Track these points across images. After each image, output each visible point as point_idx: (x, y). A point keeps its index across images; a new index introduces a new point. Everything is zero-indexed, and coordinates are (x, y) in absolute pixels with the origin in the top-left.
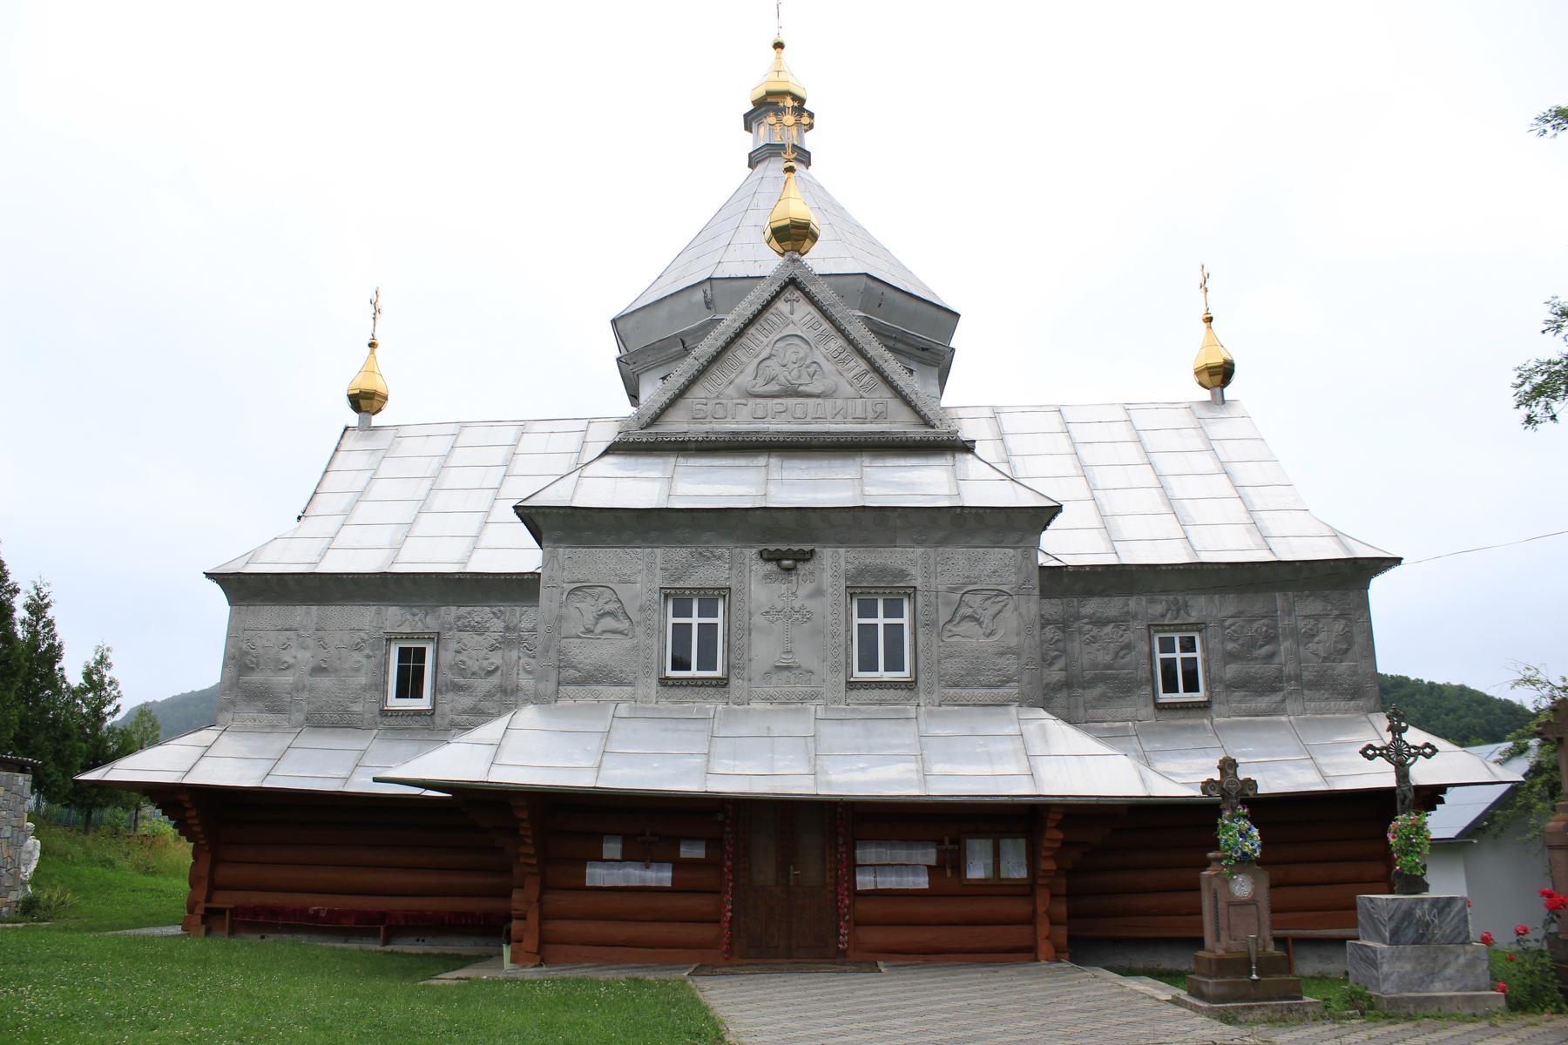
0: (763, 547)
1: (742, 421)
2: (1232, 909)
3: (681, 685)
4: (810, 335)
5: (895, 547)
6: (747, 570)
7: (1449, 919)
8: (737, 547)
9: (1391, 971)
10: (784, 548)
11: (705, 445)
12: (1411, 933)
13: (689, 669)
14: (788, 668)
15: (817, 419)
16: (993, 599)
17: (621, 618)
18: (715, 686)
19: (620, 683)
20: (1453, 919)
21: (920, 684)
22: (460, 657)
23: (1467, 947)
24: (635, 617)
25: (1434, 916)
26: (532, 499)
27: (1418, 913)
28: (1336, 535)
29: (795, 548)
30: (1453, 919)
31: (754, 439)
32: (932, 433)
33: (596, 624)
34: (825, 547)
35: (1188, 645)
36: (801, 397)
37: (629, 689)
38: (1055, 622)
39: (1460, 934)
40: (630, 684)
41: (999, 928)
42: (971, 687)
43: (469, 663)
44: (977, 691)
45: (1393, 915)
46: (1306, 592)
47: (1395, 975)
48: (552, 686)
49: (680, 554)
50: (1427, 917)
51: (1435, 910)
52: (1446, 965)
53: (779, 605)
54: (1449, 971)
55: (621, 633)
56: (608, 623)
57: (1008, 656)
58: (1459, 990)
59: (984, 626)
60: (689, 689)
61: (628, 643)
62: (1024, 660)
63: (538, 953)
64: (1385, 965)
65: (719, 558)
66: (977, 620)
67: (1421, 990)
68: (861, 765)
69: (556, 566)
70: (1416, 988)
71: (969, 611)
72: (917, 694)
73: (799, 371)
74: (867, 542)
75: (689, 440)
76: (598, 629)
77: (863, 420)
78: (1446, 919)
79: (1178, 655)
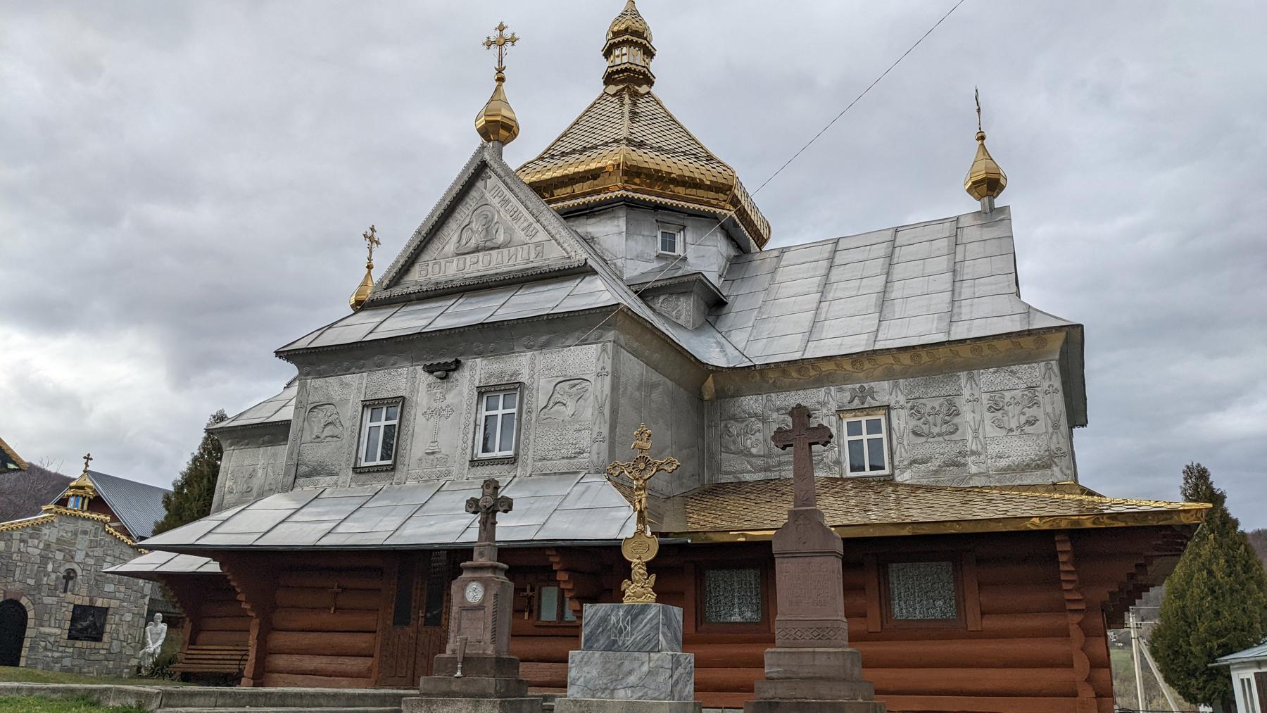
2: (464, 613)
3: (365, 472)
5: (514, 353)
6: (417, 382)
7: (641, 626)
8: (412, 366)
9: (579, 675)
12: (602, 641)
13: (375, 460)
16: (577, 387)
17: (338, 426)
18: (387, 470)
19: (331, 474)
23: (652, 654)
24: (347, 424)
25: (628, 623)
27: (613, 619)
29: (442, 361)
33: (323, 431)
34: (468, 359)
35: (874, 427)
36: (488, 250)
37: (336, 477)
38: (756, 415)
39: (649, 641)
40: (337, 474)
45: (589, 621)
46: (991, 370)
47: (582, 679)
48: (291, 478)
50: (621, 624)
51: (629, 617)
52: (630, 673)
54: (632, 679)
56: (329, 430)
57: (583, 432)
59: (569, 409)
62: (595, 435)
63: (252, 679)
64: (573, 670)
66: (565, 405)
67: (603, 696)
68: (432, 523)
70: (599, 694)
72: (517, 467)
74: (496, 353)
75: (410, 293)
76: (323, 437)
78: (638, 626)
79: (865, 437)
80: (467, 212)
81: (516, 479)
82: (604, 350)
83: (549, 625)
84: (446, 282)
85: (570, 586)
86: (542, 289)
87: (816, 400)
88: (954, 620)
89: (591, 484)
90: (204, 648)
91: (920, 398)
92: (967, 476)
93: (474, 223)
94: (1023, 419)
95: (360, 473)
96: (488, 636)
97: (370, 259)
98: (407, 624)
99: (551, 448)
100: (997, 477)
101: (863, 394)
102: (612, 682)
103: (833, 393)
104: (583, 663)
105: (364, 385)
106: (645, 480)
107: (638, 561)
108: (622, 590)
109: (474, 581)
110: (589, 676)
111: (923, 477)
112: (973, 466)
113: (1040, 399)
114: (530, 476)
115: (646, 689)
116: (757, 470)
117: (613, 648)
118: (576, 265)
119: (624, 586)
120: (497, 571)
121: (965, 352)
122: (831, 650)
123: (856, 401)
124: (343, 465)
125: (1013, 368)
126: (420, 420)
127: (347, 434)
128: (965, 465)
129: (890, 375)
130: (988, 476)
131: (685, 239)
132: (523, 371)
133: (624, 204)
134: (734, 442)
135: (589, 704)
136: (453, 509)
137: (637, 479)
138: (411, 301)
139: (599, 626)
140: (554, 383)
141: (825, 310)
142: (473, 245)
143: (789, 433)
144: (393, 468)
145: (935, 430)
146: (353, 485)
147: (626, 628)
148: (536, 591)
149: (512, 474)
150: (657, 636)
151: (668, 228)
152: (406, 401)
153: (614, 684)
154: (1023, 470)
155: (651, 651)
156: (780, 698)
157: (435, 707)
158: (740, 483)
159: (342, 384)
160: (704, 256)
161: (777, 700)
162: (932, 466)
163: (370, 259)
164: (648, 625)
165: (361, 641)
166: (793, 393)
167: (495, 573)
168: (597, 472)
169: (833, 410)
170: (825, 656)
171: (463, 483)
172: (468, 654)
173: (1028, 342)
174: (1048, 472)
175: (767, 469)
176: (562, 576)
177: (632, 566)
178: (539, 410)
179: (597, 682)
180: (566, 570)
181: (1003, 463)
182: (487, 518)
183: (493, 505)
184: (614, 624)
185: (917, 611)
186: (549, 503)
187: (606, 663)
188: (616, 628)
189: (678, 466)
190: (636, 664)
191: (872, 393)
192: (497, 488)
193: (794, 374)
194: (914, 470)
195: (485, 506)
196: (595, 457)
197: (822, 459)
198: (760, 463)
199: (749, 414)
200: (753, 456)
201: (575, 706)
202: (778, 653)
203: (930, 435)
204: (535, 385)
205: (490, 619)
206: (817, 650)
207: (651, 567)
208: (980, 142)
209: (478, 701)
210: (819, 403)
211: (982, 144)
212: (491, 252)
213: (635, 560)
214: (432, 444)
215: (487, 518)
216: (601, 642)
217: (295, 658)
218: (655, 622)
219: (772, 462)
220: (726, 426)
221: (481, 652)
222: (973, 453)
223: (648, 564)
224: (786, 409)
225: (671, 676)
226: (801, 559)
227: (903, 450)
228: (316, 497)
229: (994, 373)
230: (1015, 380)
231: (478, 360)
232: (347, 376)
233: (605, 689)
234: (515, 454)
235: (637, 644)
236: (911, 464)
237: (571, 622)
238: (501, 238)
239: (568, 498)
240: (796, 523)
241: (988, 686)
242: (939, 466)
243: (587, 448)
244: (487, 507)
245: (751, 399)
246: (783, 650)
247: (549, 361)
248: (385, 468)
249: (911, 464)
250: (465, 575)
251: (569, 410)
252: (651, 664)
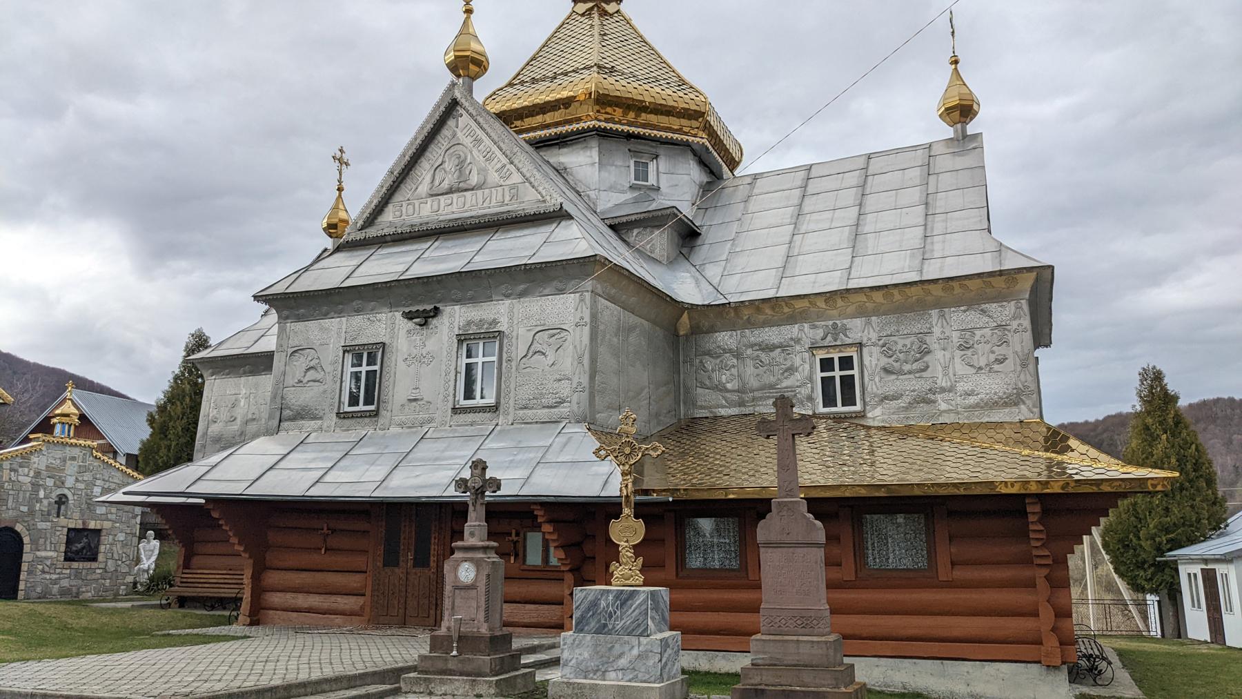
6: (397, 328)
7: (630, 611)
10: (414, 309)
11: (396, 237)
14: (415, 400)
16: (556, 337)
18: (370, 416)
19: (315, 418)
20: (634, 611)
21: (501, 409)
24: (328, 368)
26: (273, 288)
27: (603, 604)
29: (421, 308)
30: (634, 611)
31: (425, 228)
32: (542, 207)
34: (446, 306)
38: (730, 351)
40: (321, 418)
41: (546, 607)
42: (536, 409)
44: (539, 411)
45: (580, 605)
46: (962, 308)
47: (574, 661)
51: (618, 602)
52: (621, 656)
53: (415, 352)
54: (623, 662)
55: (318, 381)
56: (312, 375)
58: (630, 681)
60: (354, 420)
61: (322, 388)
63: (249, 616)
64: (566, 651)
65: (380, 321)
66: (544, 354)
67: (595, 677)
69: (284, 336)
70: (591, 675)
71: (539, 348)
73: (460, 171)
74: (474, 300)
76: (305, 381)
78: (627, 611)
79: (837, 373)
80: (440, 152)
81: (498, 428)
82: (582, 300)
83: (534, 569)
84: (421, 224)
85: (555, 537)
86: (518, 233)
87: (789, 336)
88: (925, 569)
89: (571, 435)
90: (199, 571)
91: (891, 336)
92: (936, 413)
93: (447, 163)
94: (992, 358)
95: (344, 418)
96: (481, 615)
97: (340, 181)
98: (397, 565)
99: (531, 397)
100: (966, 414)
101: (836, 331)
102: (603, 665)
103: (806, 329)
104: (575, 645)
105: (344, 330)
106: (631, 465)
107: (626, 544)
108: (611, 571)
109: (466, 561)
110: (581, 658)
111: (893, 413)
112: (942, 403)
113: (1010, 338)
114: (512, 424)
115: (636, 672)
116: (731, 404)
117: (604, 632)
118: (552, 210)
119: (612, 568)
120: (488, 551)
121: (936, 291)
122: (815, 639)
123: (829, 338)
124: (327, 410)
125: (983, 306)
126: (401, 366)
127: (329, 378)
128: (934, 402)
129: (862, 313)
130: (958, 413)
131: (658, 168)
132: (502, 320)
133: (598, 135)
134: (710, 378)
135: (581, 686)
136: (437, 459)
137: (623, 465)
138: (386, 242)
139: (589, 610)
140: (534, 333)
141: (798, 243)
142: (446, 186)
143: (772, 424)
144: (376, 414)
145: (907, 367)
146: (338, 430)
147: (615, 612)
148: (522, 535)
149: (494, 422)
150: (645, 622)
151: (641, 158)
152: (386, 347)
153: (606, 666)
154: (991, 408)
155: (641, 635)
156: (766, 685)
157: (433, 685)
158: (716, 418)
159: (322, 329)
160: (677, 185)
161: (763, 687)
162: (901, 403)
163: (340, 181)
164: (637, 611)
165: (354, 581)
166: (767, 329)
167: (486, 553)
168: (578, 422)
169: (807, 346)
170: (809, 645)
171: (445, 430)
172: (463, 632)
173: (999, 282)
174: (1015, 409)
175: (742, 404)
176: (547, 528)
177: (620, 549)
178: (519, 359)
179: (589, 664)
180: (549, 521)
181: (972, 400)
182: (477, 498)
183: (482, 486)
184: (604, 608)
185: (890, 561)
186: (532, 455)
187: (596, 645)
188: (606, 613)
189: (663, 451)
190: (627, 648)
191: (845, 330)
192: (484, 469)
193: (768, 311)
194: (885, 406)
195: (474, 487)
196: (575, 407)
197: (795, 395)
198: (735, 397)
199: (724, 350)
200: (728, 391)
201: (568, 687)
202: (763, 640)
203: (901, 372)
204: (514, 334)
205: (483, 599)
206: (801, 638)
207: (638, 550)
208: (953, 66)
209: (474, 680)
210: (792, 339)
211: (956, 69)
212: (465, 193)
213: (622, 543)
214: (414, 391)
215: (477, 498)
216: (593, 624)
217: (289, 595)
218: (644, 607)
219: (746, 397)
220: (701, 362)
221: (475, 630)
222: (943, 390)
223: (635, 547)
224: (760, 345)
225: (661, 660)
226: (786, 549)
227: (874, 386)
228: (302, 442)
229: (965, 311)
230: (986, 319)
231: (457, 308)
232: (327, 320)
233: (597, 671)
234: (497, 403)
235: (627, 629)
236: (882, 400)
237: (556, 567)
238: (474, 179)
239: (550, 450)
240: (780, 514)
241: (956, 633)
242: (909, 403)
243: (567, 397)
244: (476, 488)
245: (726, 335)
246: (768, 637)
247: (528, 310)
248: (368, 414)
249: (882, 400)
250: (458, 555)
251: (551, 358)
252: (641, 649)
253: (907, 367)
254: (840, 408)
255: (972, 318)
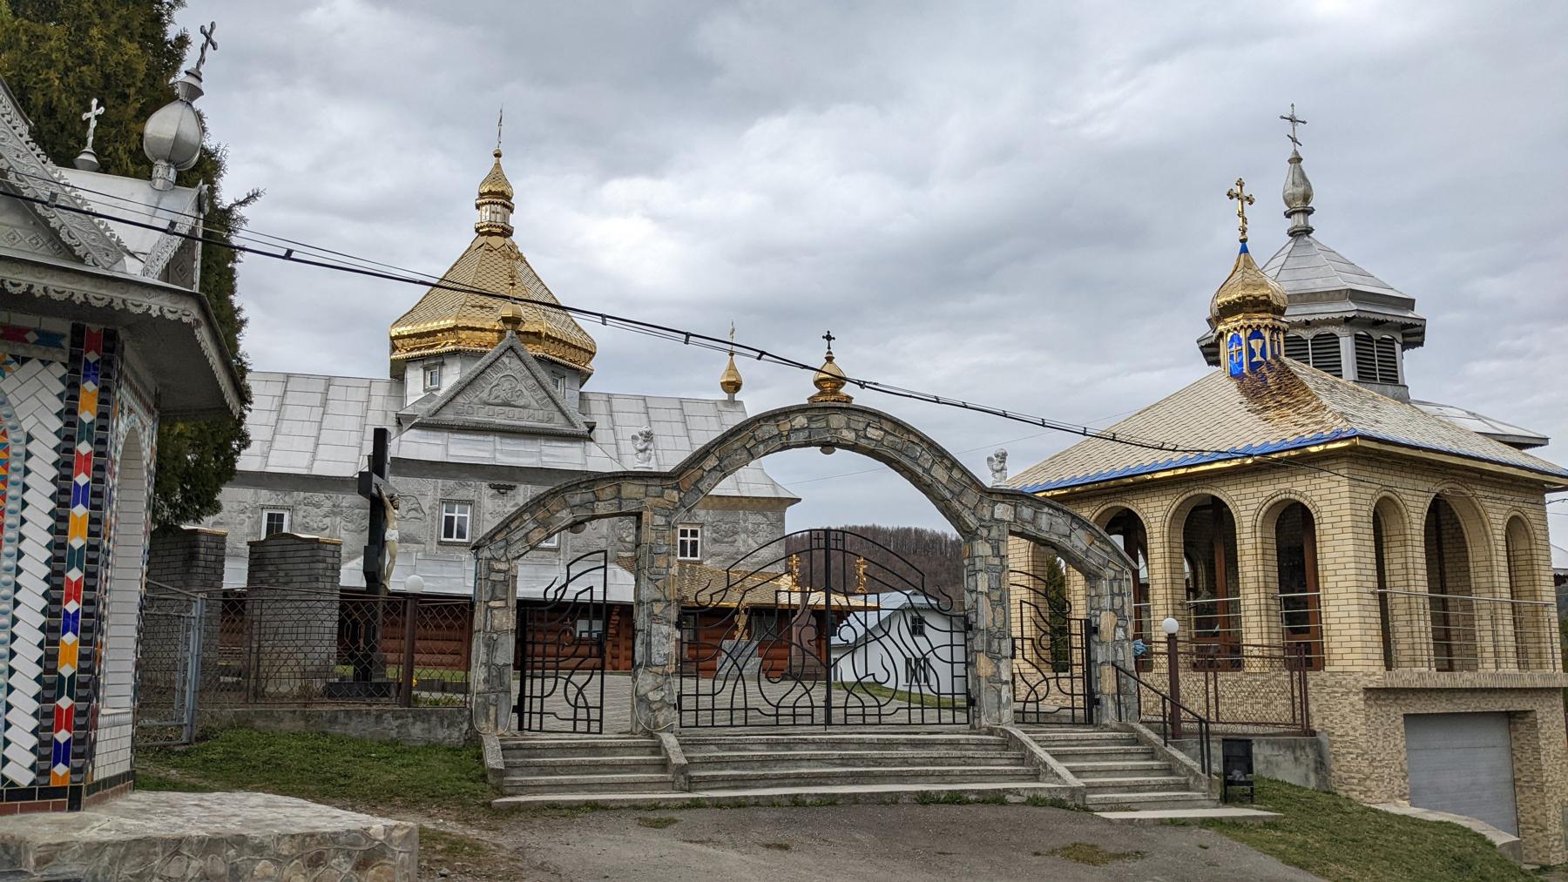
0: (492, 482)
1: (481, 416)
4: (518, 376)
15: (519, 419)
19: (418, 543)
22: (306, 520)
24: (427, 511)
28: (774, 484)
35: (694, 533)
43: (311, 523)
49: (451, 483)
53: (498, 509)
56: (412, 514)
61: (422, 524)
76: (408, 517)
77: (542, 421)
79: (689, 539)
127: (429, 519)
145: (726, 540)
146: (439, 552)
173: (775, 503)
200: (626, 542)
238: (521, 402)
253: (726, 540)
254: (689, 558)
255: (760, 518)
